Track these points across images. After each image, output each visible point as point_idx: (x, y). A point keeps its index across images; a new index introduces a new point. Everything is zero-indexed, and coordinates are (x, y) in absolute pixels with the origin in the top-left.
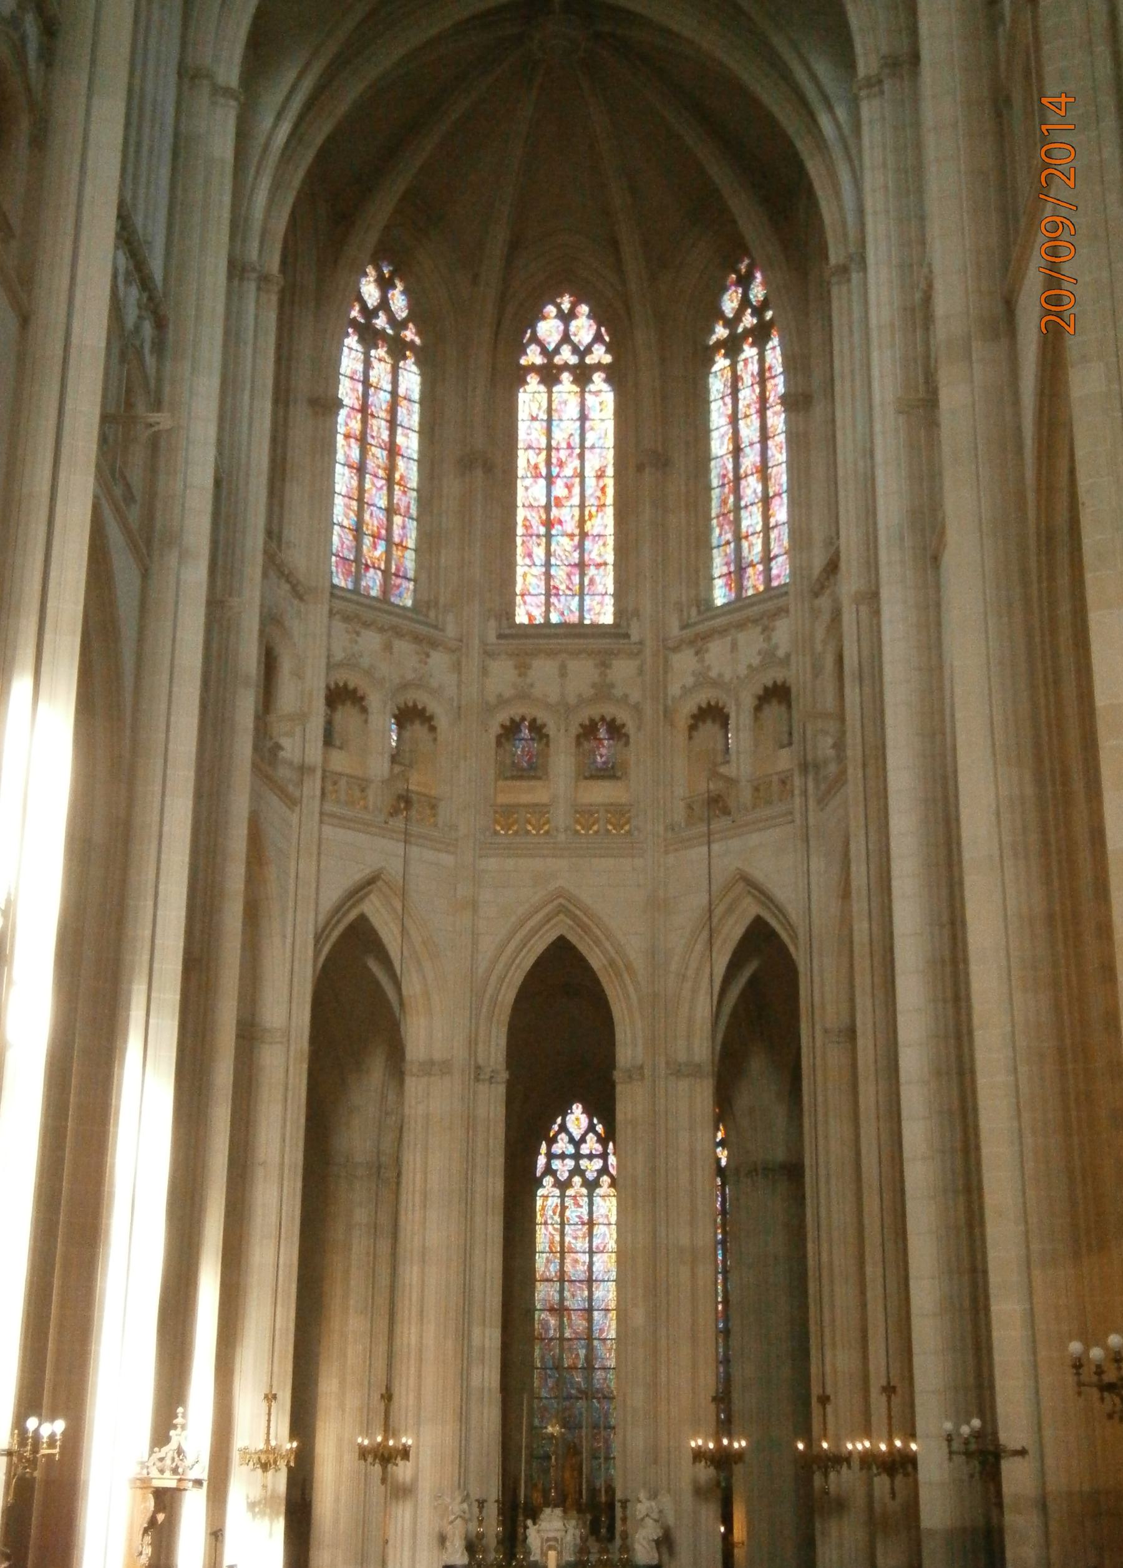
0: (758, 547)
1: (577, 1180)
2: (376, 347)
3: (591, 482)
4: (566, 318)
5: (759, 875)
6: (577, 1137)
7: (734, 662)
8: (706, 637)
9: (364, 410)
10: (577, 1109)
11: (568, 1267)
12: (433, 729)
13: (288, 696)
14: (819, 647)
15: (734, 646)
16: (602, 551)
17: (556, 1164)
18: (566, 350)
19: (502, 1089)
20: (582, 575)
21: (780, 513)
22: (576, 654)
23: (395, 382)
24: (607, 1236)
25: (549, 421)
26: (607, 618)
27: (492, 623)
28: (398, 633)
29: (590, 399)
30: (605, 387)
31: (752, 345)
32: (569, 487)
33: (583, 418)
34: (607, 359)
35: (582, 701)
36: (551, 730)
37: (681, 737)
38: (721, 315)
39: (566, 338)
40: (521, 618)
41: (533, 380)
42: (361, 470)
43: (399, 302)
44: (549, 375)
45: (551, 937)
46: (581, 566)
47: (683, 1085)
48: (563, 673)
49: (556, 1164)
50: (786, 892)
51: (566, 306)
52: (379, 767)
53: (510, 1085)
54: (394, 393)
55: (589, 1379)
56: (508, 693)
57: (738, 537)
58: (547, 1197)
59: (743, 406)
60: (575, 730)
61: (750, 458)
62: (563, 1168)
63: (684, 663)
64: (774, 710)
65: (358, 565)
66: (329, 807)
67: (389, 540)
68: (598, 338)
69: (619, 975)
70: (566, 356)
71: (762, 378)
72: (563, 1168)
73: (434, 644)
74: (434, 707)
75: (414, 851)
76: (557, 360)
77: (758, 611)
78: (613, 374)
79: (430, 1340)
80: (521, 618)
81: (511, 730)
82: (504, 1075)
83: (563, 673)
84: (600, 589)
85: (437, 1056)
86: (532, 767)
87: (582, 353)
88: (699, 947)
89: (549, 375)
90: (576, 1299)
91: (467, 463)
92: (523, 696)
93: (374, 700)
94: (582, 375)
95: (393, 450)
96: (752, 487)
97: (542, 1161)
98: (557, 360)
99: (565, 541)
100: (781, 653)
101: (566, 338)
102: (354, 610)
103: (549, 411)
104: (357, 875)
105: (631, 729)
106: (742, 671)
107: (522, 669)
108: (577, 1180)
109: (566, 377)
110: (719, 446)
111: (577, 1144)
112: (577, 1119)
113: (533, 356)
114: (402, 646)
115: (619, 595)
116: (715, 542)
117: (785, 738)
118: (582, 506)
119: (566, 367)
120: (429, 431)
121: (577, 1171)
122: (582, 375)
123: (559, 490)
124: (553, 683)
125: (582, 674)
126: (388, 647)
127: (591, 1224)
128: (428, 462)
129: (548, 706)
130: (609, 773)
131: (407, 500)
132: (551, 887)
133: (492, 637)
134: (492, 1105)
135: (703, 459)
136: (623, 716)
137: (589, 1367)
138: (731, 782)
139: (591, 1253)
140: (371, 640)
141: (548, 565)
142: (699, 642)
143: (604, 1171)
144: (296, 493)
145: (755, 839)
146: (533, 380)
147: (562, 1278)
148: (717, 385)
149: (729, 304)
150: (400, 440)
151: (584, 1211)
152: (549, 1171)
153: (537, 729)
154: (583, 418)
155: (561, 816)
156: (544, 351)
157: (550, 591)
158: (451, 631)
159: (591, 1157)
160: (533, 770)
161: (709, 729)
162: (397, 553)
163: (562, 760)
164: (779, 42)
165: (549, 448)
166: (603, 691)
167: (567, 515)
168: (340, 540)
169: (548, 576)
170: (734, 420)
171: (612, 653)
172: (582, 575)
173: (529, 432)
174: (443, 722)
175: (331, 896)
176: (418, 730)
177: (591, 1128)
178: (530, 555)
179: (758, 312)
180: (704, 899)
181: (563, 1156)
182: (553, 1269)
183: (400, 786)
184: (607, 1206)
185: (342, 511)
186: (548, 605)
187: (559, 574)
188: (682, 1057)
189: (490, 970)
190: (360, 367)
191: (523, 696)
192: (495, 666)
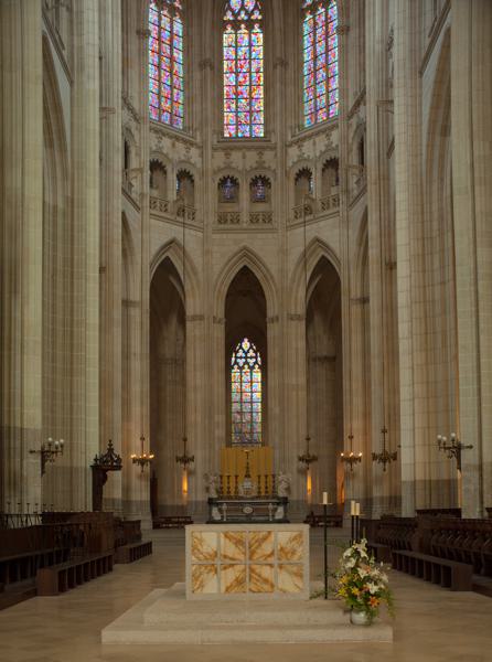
0: (324, 101)
1: (246, 366)
2: (163, 9)
3: (254, 75)
5: (324, 239)
6: (246, 350)
7: (313, 151)
8: (304, 139)
9: (159, 39)
10: (246, 340)
11: (244, 397)
12: (193, 181)
13: (134, 164)
14: (350, 141)
15: (314, 144)
16: (260, 105)
17: (238, 360)
19: (223, 326)
20: (251, 117)
21: (335, 84)
22: (249, 149)
23: (171, 27)
24: (258, 387)
25: (236, 46)
26: (262, 135)
27: (215, 136)
28: (177, 138)
29: (253, 37)
30: (259, 30)
31: (323, 7)
32: (245, 77)
33: (250, 45)
35: (252, 169)
36: (240, 181)
37: (292, 184)
40: (227, 135)
41: (229, 30)
42: (159, 67)
44: (236, 25)
45: (242, 266)
46: (250, 112)
47: (294, 323)
48: (244, 157)
49: (238, 360)
50: (334, 245)
52: (172, 196)
53: (226, 323)
55: (252, 436)
56: (222, 166)
57: (315, 98)
58: (235, 373)
59: (318, 38)
60: (249, 180)
61: (321, 61)
62: (241, 362)
63: (293, 152)
64: (330, 171)
65: (160, 110)
66: (153, 212)
67: (171, 99)
69: (268, 281)
70: (243, 16)
71: (327, 21)
72: (241, 362)
73: (192, 144)
75: (187, 231)
76: (239, 18)
77: (327, 129)
78: (263, 25)
79: (199, 419)
80: (227, 135)
81: (223, 182)
82: (224, 320)
83: (244, 157)
84: (258, 121)
85: (198, 313)
86: (232, 198)
87: (250, 14)
88: (299, 270)
89: (236, 25)
90: (247, 408)
91: (203, 65)
92: (228, 167)
94: (250, 24)
95: (172, 59)
96: (321, 74)
97: (233, 359)
98: (239, 18)
99: (243, 101)
100: (334, 145)
102: (159, 131)
104: (165, 240)
105: (272, 180)
106: (318, 154)
107: (227, 155)
108: (246, 366)
109: (243, 26)
110: (307, 57)
111: (246, 353)
112: (246, 344)
113: (229, 17)
114: (180, 145)
115: (265, 125)
116: (305, 100)
117: (334, 183)
118: (250, 85)
119: (243, 21)
120: (186, 51)
121: (247, 363)
122: (250, 24)
123: (241, 79)
126: (173, 145)
127: (251, 382)
128: (187, 66)
129: (239, 172)
130: (263, 200)
131: (179, 82)
132: (242, 245)
133: (215, 143)
134: (219, 332)
135: (300, 64)
136: (269, 175)
137: (251, 433)
138: (313, 200)
139: (252, 392)
140: (166, 142)
141: (237, 112)
142: (299, 142)
143: (256, 363)
144: (134, 74)
145: (322, 224)
146: (229, 30)
147: (241, 401)
148: (306, 28)
150: (175, 54)
151: (249, 378)
152: (236, 363)
153: (234, 182)
154: (250, 45)
155: (245, 217)
156: (233, 14)
157: (238, 124)
158: (198, 137)
159: (251, 358)
161: (303, 180)
162: (175, 105)
163: (244, 193)
166: (261, 165)
167: (244, 89)
168: (152, 99)
169: (237, 116)
170: (314, 44)
171: (264, 148)
172: (251, 117)
173: (228, 52)
174: (196, 178)
175: (155, 248)
176: (186, 182)
177: (251, 347)
178: (229, 107)
180: (302, 249)
181: (241, 358)
182: (238, 399)
183: (181, 203)
184: (258, 376)
185: (152, 86)
186: (237, 129)
187: (242, 115)
188: (293, 313)
189: (217, 280)
190: (157, 19)
191: (228, 167)
192: (216, 154)
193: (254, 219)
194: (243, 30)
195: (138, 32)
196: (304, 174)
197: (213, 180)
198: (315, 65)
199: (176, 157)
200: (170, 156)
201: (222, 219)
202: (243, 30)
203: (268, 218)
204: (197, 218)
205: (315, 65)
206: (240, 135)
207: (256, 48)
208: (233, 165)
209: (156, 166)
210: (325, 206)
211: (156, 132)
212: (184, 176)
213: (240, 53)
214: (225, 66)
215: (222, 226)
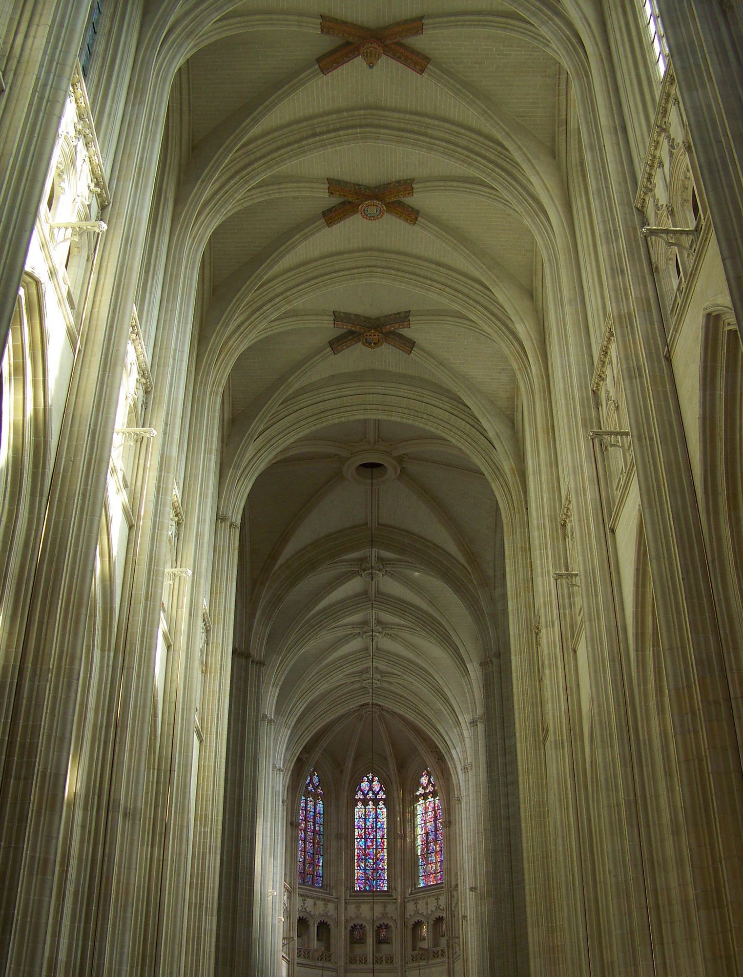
4: (371, 782)
12: (329, 929)
15: (427, 904)
18: (371, 795)
23: (315, 809)
25: (365, 818)
26: (386, 889)
28: (318, 898)
33: (377, 817)
34: (384, 796)
38: (421, 785)
39: (371, 789)
41: (360, 805)
42: (305, 841)
43: (316, 779)
44: (365, 803)
51: (370, 777)
54: (315, 812)
63: (410, 907)
68: (381, 789)
70: (371, 795)
73: (329, 901)
74: (330, 922)
81: (354, 928)
87: (376, 794)
89: (365, 803)
92: (358, 917)
93: (311, 922)
94: (376, 802)
101: (371, 789)
103: (365, 815)
106: (429, 912)
113: (360, 796)
114: (320, 903)
118: (376, 849)
122: (376, 802)
124: (366, 912)
125: (378, 909)
126: (315, 904)
136: (391, 923)
140: (310, 902)
141: (365, 869)
145: (433, 969)
146: (360, 805)
148: (420, 809)
149: (424, 780)
150: (317, 828)
156: (363, 794)
157: (367, 879)
160: (361, 941)
164: (439, 727)
165: (365, 828)
174: (332, 927)
179: (433, 786)
193: (377, 960)
194: (371, 805)
195: (292, 824)
196: (418, 925)
197: (346, 928)
198: (427, 838)
199: (317, 913)
200: (312, 913)
201: (352, 960)
202: (371, 805)
203: (390, 960)
204: (332, 960)
205: (427, 838)
206: (368, 888)
207: (381, 820)
208: (363, 916)
209: (303, 922)
210: (436, 955)
211: (301, 895)
212: (323, 927)
213: (368, 824)
214: (356, 834)
215: (353, 966)
